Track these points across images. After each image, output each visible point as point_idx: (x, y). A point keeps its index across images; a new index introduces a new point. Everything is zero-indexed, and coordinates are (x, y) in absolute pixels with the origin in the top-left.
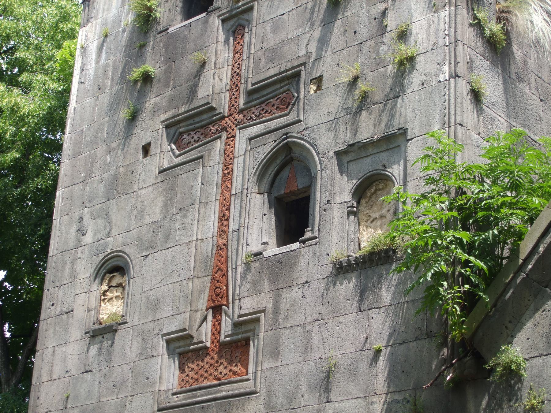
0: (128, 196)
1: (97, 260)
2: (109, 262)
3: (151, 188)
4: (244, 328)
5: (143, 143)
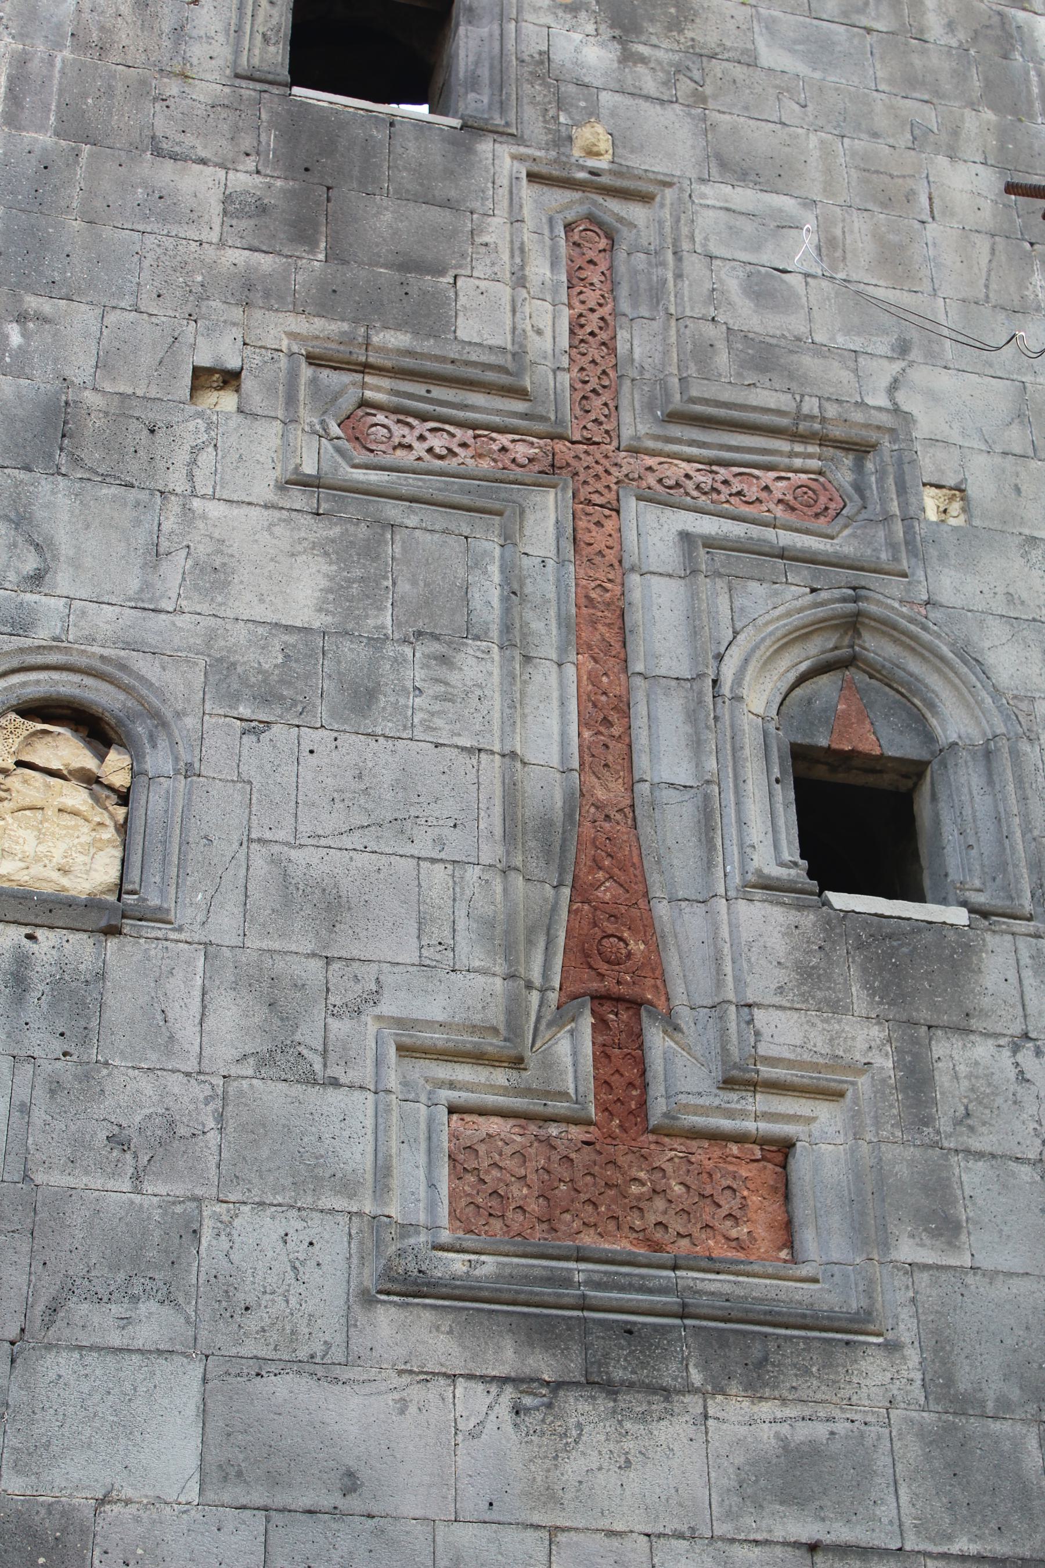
0: (133, 494)
2: (33, 676)
3: (254, 512)
4: (762, 1102)
5: (204, 360)
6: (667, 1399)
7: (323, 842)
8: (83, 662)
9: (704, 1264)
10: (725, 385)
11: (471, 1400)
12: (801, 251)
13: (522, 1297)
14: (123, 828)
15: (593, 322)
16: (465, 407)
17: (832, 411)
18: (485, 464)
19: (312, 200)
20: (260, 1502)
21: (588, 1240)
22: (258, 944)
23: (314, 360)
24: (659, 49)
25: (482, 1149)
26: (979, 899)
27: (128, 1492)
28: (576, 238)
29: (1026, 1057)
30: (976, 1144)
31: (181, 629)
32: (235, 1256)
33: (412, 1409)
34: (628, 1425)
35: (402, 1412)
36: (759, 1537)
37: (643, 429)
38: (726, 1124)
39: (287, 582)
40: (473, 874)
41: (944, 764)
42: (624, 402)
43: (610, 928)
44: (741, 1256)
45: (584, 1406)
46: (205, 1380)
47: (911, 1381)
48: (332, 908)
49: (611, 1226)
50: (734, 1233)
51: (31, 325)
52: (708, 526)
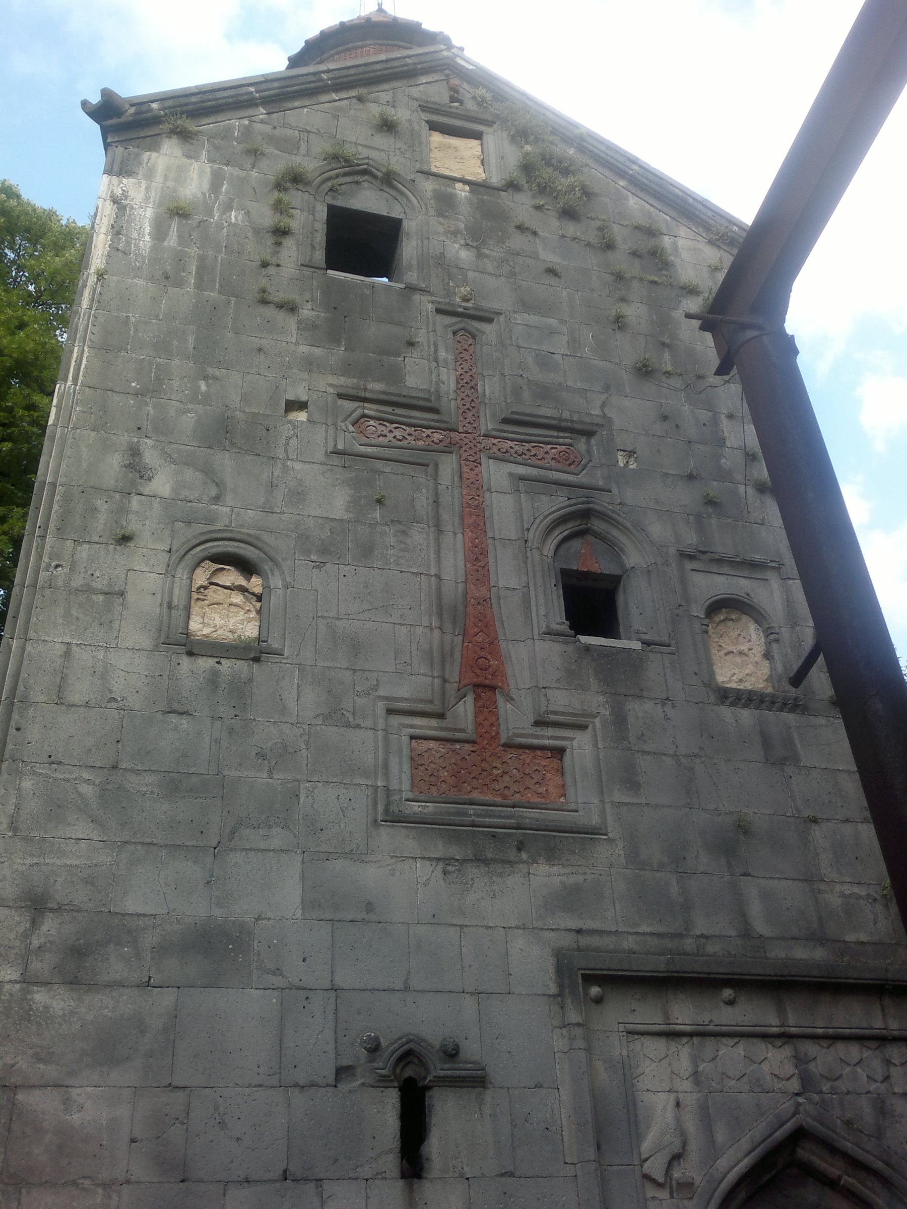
1: (186, 534)
2: (216, 543)
3: (316, 466)
4: (550, 732)
5: (291, 397)
6: (512, 866)
7: (351, 617)
8: (239, 537)
9: (526, 805)
10: (529, 406)
11: (423, 870)
12: (560, 345)
13: (445, 822)
14: (259, 612)
15: (467, 378)
16: (410, 417)
17: (576, 417)
18: (421, 443)
19: (338, 325)
20: (329, 918)
21: (475, 795)
22: (322, 664)
23: (341, 396)
24: (494, 251)
25: (426, 755)
26: (646, 637)
27: (269, 915)
28: (458, 339)
29: (668, 709)
30: (646, 748)
31: (283, 521)
32: (315, 806)
33: (398, 873)
34: (494, 878)
35: (393, 875)
36: (554, 927)
37: (490, 427)
38: (535, 742)
39: (331, 500)
40: (419, 630)
41: (628, 576)
42: (482, 414)
43: (483, 654)
44: (543, 800)
45: (475, 870)
46: (303, 862)
47: (620, 855)
48: (356, 647)
49: (485, 788)
50: (540, 790)
51: (210, 381)
52: (521, 470)
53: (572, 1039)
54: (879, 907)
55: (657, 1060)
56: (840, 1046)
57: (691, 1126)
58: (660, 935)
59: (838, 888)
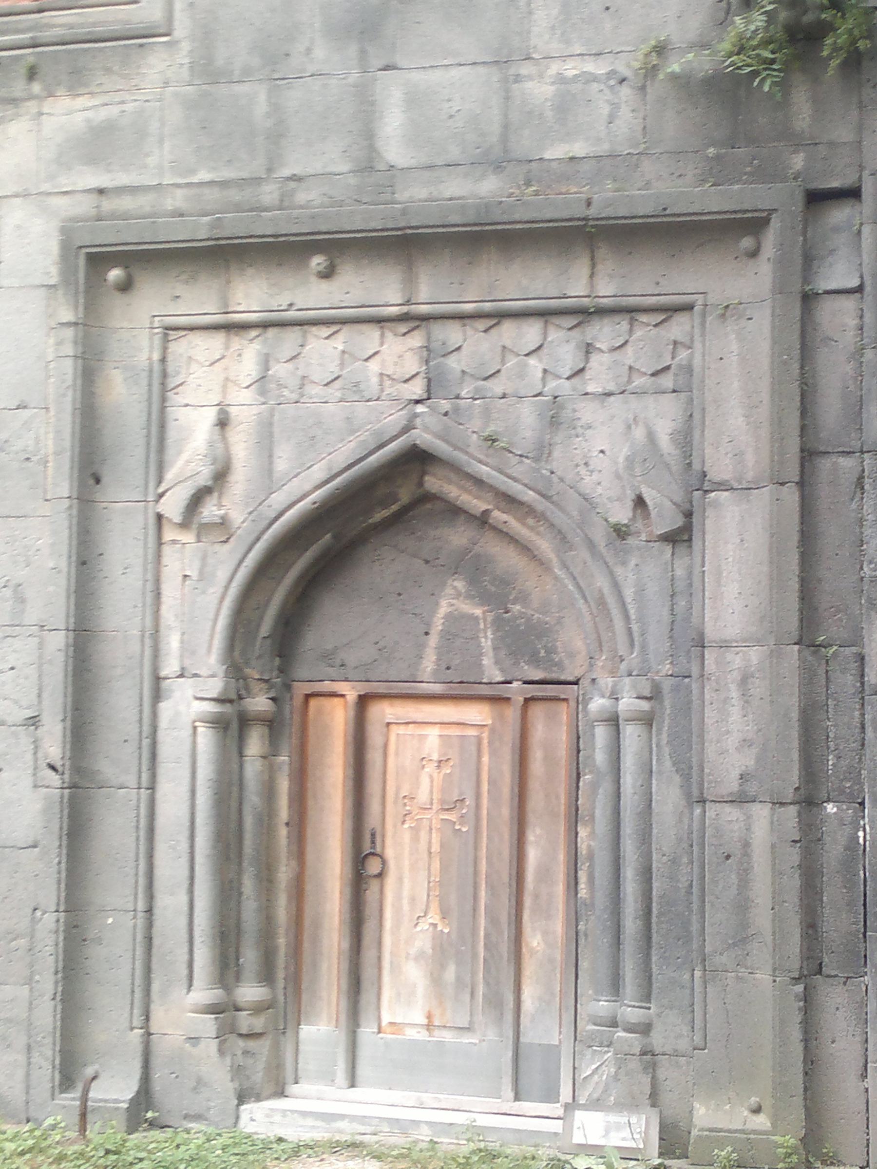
53: (59, 343)
54: (625, 91)
55: (207, 363)
56: (508, 328)
57: (241, 448)
58: (223, 184)
59: (554, 68)
